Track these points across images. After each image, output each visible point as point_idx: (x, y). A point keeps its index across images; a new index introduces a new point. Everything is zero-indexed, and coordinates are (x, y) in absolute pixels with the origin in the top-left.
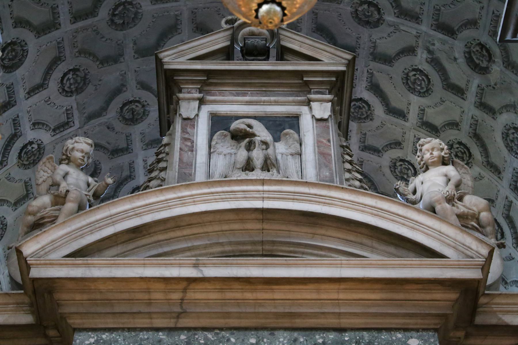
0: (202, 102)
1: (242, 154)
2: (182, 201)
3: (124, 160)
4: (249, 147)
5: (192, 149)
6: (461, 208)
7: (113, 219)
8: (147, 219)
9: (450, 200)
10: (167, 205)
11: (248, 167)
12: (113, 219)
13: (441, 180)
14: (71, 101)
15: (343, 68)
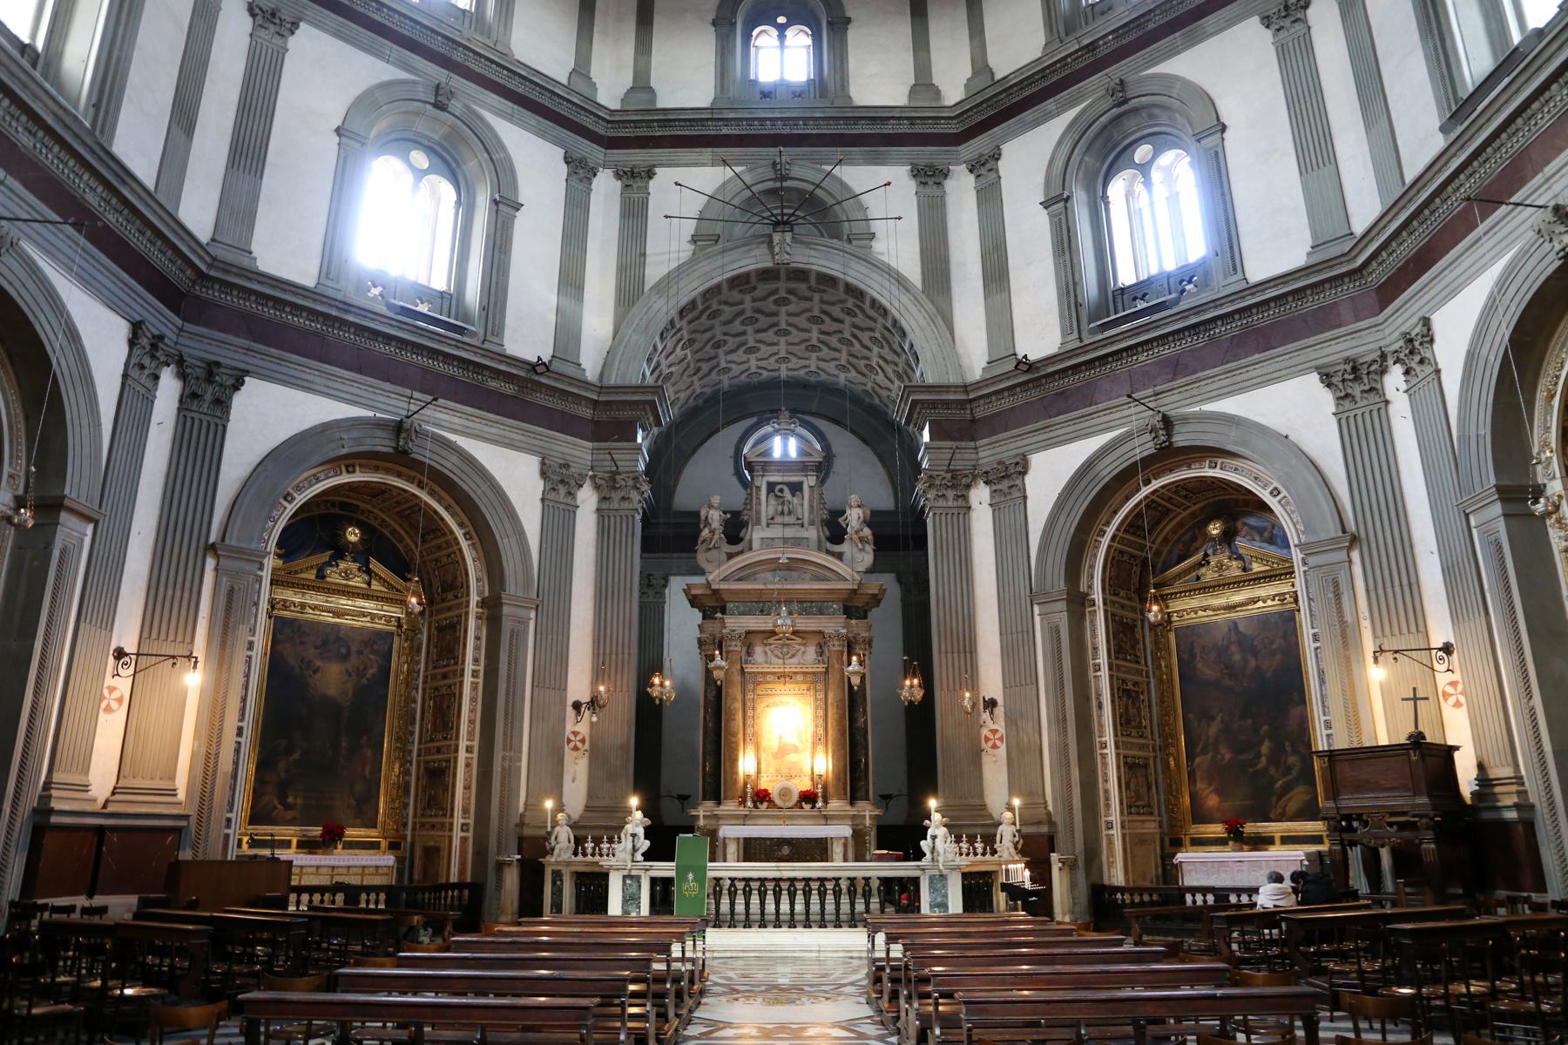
0: (763, 476)
1: (780, 508)
2: (759, 555)
3: (715, 362)
4: (783, 503)
5: (760, 504)
6: (861, 534)
7: (735, 564)
8: (747, 562)
9: (857, 532)
10: (754, 557)
11: (782, 513)
12: (735, 564)
13: (856, 517)
14: (688, 351)
15: (821, 460)
